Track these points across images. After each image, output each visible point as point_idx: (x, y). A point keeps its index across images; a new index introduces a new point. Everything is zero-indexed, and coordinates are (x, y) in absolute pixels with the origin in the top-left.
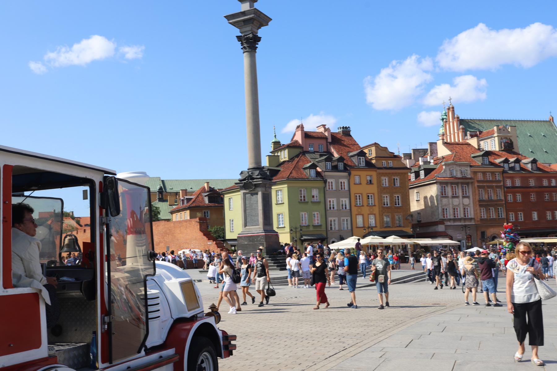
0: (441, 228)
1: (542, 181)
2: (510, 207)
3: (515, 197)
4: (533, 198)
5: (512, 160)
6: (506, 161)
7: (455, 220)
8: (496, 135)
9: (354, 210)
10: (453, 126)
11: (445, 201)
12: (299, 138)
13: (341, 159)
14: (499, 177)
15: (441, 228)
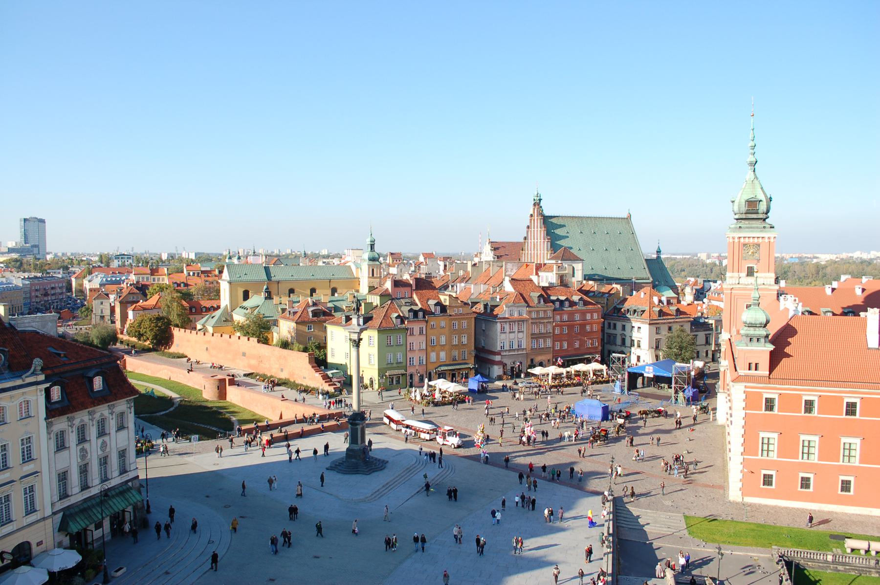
0: (497, 358)
1: (585, 316)
2: (556, 338)
3: (562, 330)
4: (577, 329)
5: (562, 298)
6: (558, 300)
7: (509, 351)
8: (555, 272)
9: (429, 349)
10: (538, 221)
11: (503, 335)
12: (388, 285)
13: (421, 310)
14: (550, 314)
15: (497, 358)
